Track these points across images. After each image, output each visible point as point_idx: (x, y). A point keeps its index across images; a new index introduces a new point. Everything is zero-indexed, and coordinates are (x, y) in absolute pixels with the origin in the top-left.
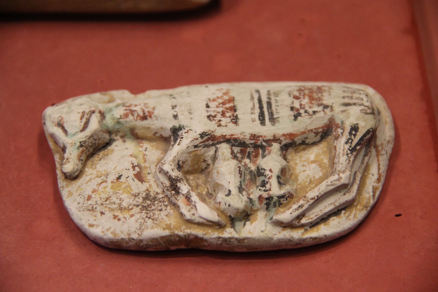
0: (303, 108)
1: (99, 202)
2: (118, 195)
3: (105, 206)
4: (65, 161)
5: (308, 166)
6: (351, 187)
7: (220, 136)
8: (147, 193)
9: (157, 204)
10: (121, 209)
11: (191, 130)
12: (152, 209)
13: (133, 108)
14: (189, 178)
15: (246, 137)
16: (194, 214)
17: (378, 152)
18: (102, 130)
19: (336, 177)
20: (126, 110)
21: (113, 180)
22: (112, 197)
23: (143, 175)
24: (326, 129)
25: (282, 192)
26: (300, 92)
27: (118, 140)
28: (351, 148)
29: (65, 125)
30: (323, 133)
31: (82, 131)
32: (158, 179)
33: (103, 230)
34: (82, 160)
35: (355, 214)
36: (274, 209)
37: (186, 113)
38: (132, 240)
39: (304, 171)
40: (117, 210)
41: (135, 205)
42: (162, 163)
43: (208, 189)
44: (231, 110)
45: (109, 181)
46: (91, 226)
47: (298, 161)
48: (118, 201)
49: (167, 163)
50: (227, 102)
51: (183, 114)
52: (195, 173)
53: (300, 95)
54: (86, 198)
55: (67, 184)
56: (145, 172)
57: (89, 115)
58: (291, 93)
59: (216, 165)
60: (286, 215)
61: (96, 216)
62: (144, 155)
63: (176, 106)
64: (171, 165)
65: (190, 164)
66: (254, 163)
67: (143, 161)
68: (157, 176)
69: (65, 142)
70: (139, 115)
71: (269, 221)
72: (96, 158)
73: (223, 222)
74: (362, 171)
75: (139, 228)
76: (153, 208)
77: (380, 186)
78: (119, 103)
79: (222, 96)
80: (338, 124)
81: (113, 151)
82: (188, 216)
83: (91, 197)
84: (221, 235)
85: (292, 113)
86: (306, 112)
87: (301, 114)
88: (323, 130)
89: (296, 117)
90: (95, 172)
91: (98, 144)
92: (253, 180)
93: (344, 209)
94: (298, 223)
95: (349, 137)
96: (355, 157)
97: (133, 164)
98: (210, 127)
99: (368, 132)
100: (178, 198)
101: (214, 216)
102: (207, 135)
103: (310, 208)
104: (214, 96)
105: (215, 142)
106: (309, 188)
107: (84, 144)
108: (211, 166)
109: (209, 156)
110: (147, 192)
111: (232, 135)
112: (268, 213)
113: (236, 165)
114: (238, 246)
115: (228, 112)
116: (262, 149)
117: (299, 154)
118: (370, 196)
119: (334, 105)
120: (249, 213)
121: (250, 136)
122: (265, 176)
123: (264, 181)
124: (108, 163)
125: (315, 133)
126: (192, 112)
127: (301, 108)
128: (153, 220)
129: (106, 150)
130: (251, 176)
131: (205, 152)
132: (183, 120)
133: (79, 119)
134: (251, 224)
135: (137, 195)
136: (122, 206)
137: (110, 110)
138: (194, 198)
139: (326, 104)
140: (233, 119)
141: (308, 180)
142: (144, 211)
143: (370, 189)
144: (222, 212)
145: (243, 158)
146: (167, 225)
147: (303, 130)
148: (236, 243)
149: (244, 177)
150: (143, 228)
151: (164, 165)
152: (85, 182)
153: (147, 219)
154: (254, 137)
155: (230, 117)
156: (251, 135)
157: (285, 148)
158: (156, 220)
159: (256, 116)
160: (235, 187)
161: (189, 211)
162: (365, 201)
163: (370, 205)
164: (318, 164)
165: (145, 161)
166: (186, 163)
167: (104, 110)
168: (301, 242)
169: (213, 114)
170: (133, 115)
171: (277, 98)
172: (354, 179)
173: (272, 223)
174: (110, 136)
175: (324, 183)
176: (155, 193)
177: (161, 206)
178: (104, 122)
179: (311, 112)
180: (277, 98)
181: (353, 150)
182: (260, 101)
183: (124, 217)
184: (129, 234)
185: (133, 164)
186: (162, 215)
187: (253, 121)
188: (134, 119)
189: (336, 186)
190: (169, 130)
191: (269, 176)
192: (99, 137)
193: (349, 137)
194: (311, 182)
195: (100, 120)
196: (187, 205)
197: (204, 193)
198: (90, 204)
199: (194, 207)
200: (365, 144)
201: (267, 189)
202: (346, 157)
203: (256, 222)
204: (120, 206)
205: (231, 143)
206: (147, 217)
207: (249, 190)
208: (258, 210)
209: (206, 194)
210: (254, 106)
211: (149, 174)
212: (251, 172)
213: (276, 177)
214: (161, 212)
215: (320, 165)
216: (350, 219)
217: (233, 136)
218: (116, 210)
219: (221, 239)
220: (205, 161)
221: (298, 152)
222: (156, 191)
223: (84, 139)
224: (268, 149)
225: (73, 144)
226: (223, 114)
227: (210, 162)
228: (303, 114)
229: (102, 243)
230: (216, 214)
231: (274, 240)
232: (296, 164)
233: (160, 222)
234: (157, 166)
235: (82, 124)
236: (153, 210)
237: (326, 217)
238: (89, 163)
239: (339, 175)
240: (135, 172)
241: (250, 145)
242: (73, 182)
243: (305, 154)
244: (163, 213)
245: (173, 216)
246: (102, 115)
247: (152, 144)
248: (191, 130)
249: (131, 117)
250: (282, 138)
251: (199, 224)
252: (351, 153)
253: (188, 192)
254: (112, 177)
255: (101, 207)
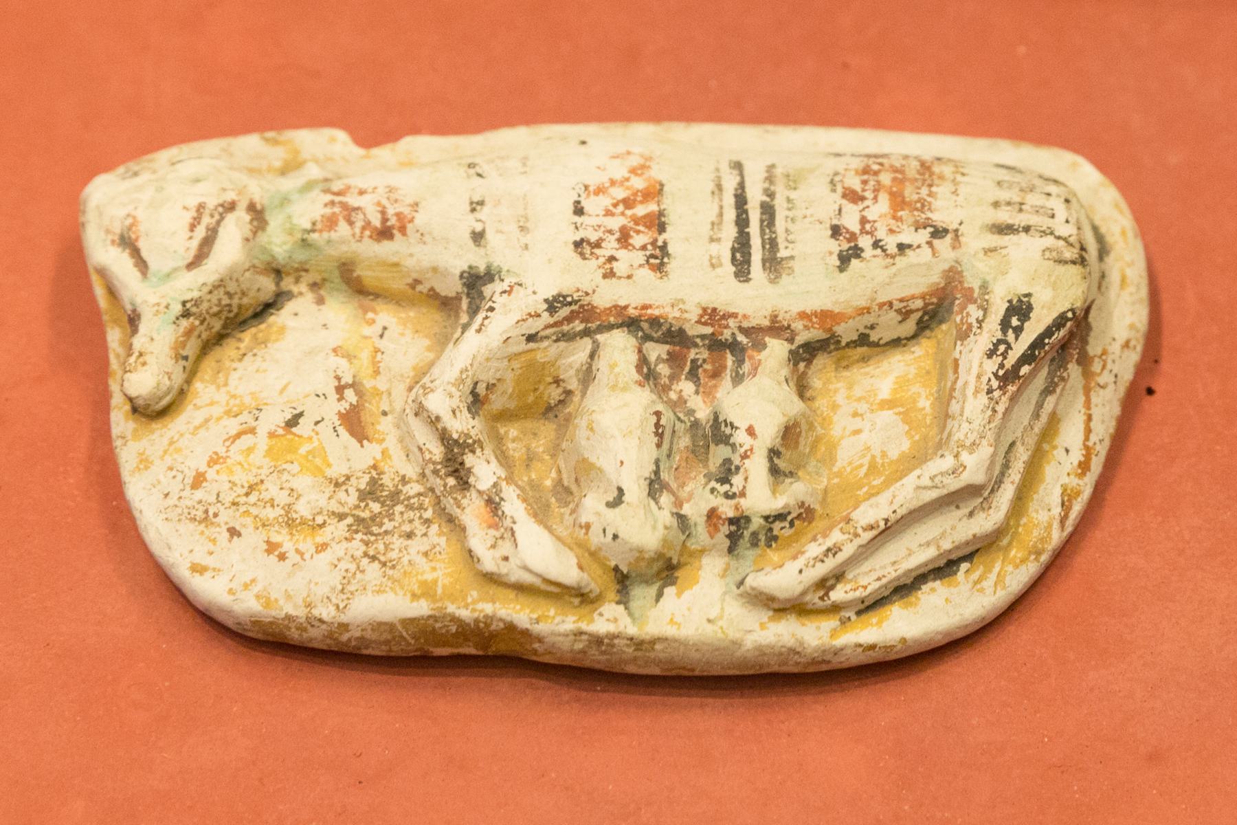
0: (867, 233)
1: (228, 498)
2: (285, 476)
3: (243, 509)
4: (132, 360)
5: (868, 412)
6: (992, 491)
7: (610, 309)
8: (372, 479)
9: (402, 513)
10: (291, 523)
11: (520, 285)
12: (384, 528)
13: (353, 200)
14: (506, 432)
15: (686, 315)
16: (506, 559)
17: (1087, 374)
18: (254, 266)
19: (948, 462)
20: (332, 203)
21: (273, 428)
22: (267, 485)
23: (366, 417)
24: (935, 300)
25: (777, 504)
26: (865, 177)
27: (301, 294)
28: (1001, 373)
29: (141, 244)
30: (925, 313)
31: (191, 266)
32: (410, 434)
33: (233, 585)
34: (186, 358)
35: (999, 574)
36: (751, 554)
37: (513, 228)
38: (316, 623)
39: (857, 432)
40: (280, 523)
41: (333, 513)
42: (424, 387)
43: (559, 471)
44: (647, 228)
45: (263, 428)
46: (198, 569)
47: (840, 398)
48: (282, 498)
49: (440, 390)
50: (639, 199)
51: (501, 232)
52: (526, 417)
53: (864, 190)
54: (189, 481)
55: (135, 430)
56: (372, 407)
57: (217, 217)
58: (837, 179)
59: (589, 402)
60: (786, 574)
61: (214, 541)
62: (377, 351)
63: (481, 203)
64: (451, 396)
65: (510, 390)
66: (709, 394)
67: (370, 371)
68: (407, 424)
69: (139, 300)
70: (368, 224)
71: (734, 588)
72: (229, 350)
73: (593, 585)
74: (1031, 440)
75: (340, 587)
76: (388, 525)
77: (1086, 486)
78: (311, 174)
79: (628, 180)
80: (971, 290)
81: (282, 330)
82: (489, 563)
83: (205, 480)
84: (584, 626)
85: (835, 246)
86: (876, 244)
87: (862, 250)
88: (926, 305)
89: (844, 260)
90: (222, 397)
91: (240, 307)
92: (699, 452)
93: (969, 557)
94: (821, 598)
95: (999, 335)
96: (1013, 399)
97: (338, 378)
98: (581, 278)
99: (1060, 321)
100: (465, 502)
101: (566, 569)
102: (570, 304)
103: (862, 554)
104: (603, 179)
105: (593, 326)
106: (865, 489)
107: (194, 310)
108: (576, 399)
109: (570, 366)
110: (374, 473)
111: (645, 307)
112: (733, 563)
113: (646, 409)
114: (635, 659)
115: (638, 232)
116: (732, 353)
117: (846, 373)
118: (1052, 518)
119: (962, 228)
120: (675, 561)
121: (701, 312)
122: (733, 446)
123: (728, 461)
124: (265, 371)
125: (899, 311)
126: (528, 225)
127: (863, 231)
128: (384, 564)
129: (263, 326)
130: (694, 437)
131: (560, 356)
132: (499, 252)
133: (187, 228)
134: (679, 594)
135: (344, 483)
136: (295, 516)
137: (285, 201)
138: (513, 506)
139: (939, 224)
140: (653, 256)
141: (866, 461)
142: (359, 536)
143: (1055, 498)
144: (594, 554)
145: (673, 378)
146: (424, 584)
147: (863, 303)
148: (631, 650)
149: (672, 443)
150: (351, 588)
151: (430, 396)
152: (191, 427)
153: (365, 561)
154: (711, 315)
155: (644, 248)
156: (705, 310)
157: (805, 354)
158: (393, 567)
159: (724, 250)
160: (639, 478)
161: (493, 546)
162: (1035, 533)
163: (1050, 548)
164: (900, 413)
165: (377, 372)
166: (500, 388)
167: (266, 202)
168: (827, 658)
169: (593, 238)
170: (351, 223)
171: (793, 195)
172: (1006, 466)
173: (741, 595)
174: (277, 284)
175: (910, 481)
176: (397, 479)
177: (411, 521)
178: (263, 238)
179: (892, 249)
180: (793, 195)
181: (1008, 377)
182: (741, 201)
183: (297, 551)
184: (309, 605)
185: (338, 378)
186: (413, 551)
187: (713, 266)
188: (354, 235)
189: (945, 492)
190: (457, 277)
191: (746, 447)
192: (244, 286)
193: (999, 335)
194: (873, 469)
195: (249, 234)
196: (490, 527)
197: (548, 483)
198: (200, 502)
199: (508, 535)
200: (1049, 357)
201: (734, 489)
202: (983, 399)
203: (696, 588)
204: (287, 513)
205: (642, 330)
206: (366, 554)
207: (683, 485)
208: (702, 551)
209: (555, 487)
210: (721, 215)
211: (385, 413)
212: (696, 424)
213: (765, 453)
214: (409, 542)
215: (906, 417)
216: (982, 590)
217: (649, 311)
218: (277, 527)
219: (584, 637)
220: (557, 381)
221: (846, 367)
222: (402, 472)
223: (196, 294)
224: (751, 358)
225: (162, 308)
226: (624, 238)
227: (573, 385)
228: (869, 252)
229: (230, 623)
230: (574, 561)
231: (744, 649)
232: (835, 407)
233: (405, 572)
234: (410, 389)
235: (195, 244)
236: (386, 532)
237: (908, 581)
238: (208, 365)
239: (956, 456)
240: (344, 406)
241: (698, 340)
242: (154, 426)
243: (867, 374)
244: (417, 545)
245: (443, 556)
246: (258, 215)
247: (403, 315)
248: (520, 285)
249: (343, 228)
250: (798, 325)
251: (521, 589)
252: (1000, 388)
253: (495, 485)
254: (274, 418)
255: (230, 511)
